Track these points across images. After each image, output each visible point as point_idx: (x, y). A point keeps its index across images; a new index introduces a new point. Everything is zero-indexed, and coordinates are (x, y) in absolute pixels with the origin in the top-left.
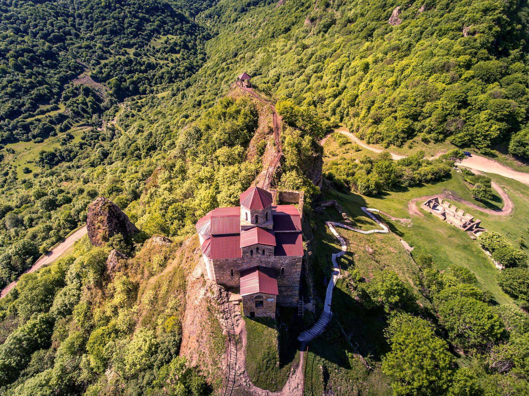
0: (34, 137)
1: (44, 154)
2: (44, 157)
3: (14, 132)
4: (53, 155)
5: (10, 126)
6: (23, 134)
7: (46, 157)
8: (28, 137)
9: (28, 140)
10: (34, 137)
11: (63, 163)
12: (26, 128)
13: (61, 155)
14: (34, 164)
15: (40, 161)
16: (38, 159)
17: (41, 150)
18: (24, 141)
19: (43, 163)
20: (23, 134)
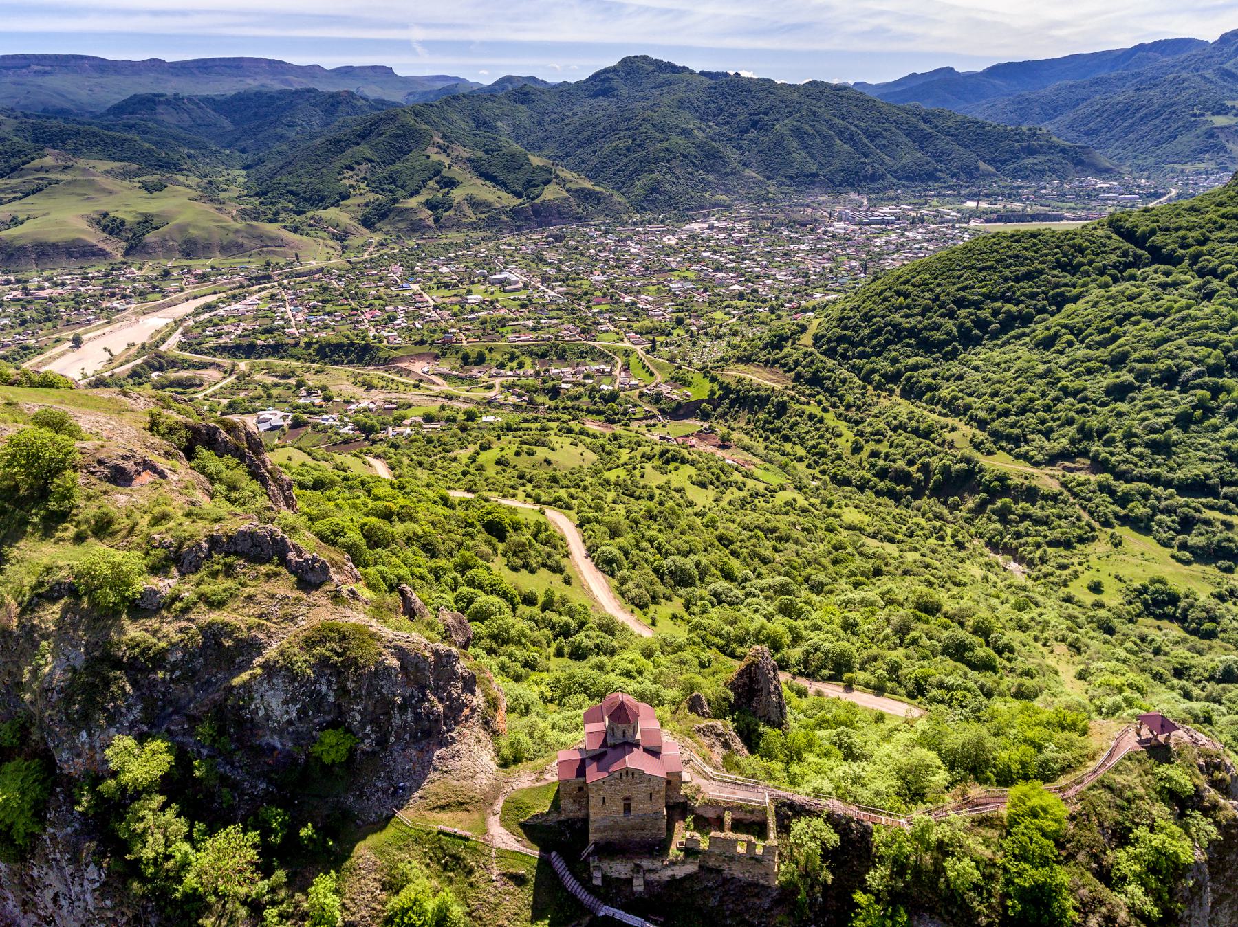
0: (1183, 546)
1: (1158, 585)
2: (1152, 588)
3: (1159, 517)
4: (1173, 599)
5: (1164, 503)
6: (1170, 528)
7: (1154, 592)
8: (1173, 539)
9: (1165, 544)
10: (1183, 546)
11: (1176, 625)
12: (1187, 524)
13: (1185, 610)
14: (1122, 586)
15: (1135, 590)
16: (1137, 584)
17: (1162, 575)
18: (1158, 541)
19: (1137, 596)
20: (1170, 528)
